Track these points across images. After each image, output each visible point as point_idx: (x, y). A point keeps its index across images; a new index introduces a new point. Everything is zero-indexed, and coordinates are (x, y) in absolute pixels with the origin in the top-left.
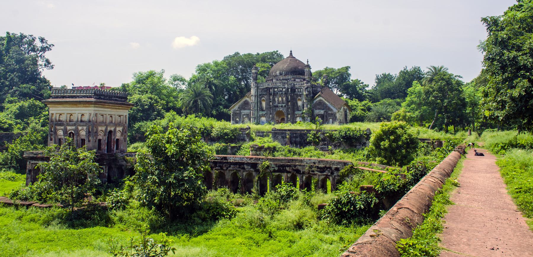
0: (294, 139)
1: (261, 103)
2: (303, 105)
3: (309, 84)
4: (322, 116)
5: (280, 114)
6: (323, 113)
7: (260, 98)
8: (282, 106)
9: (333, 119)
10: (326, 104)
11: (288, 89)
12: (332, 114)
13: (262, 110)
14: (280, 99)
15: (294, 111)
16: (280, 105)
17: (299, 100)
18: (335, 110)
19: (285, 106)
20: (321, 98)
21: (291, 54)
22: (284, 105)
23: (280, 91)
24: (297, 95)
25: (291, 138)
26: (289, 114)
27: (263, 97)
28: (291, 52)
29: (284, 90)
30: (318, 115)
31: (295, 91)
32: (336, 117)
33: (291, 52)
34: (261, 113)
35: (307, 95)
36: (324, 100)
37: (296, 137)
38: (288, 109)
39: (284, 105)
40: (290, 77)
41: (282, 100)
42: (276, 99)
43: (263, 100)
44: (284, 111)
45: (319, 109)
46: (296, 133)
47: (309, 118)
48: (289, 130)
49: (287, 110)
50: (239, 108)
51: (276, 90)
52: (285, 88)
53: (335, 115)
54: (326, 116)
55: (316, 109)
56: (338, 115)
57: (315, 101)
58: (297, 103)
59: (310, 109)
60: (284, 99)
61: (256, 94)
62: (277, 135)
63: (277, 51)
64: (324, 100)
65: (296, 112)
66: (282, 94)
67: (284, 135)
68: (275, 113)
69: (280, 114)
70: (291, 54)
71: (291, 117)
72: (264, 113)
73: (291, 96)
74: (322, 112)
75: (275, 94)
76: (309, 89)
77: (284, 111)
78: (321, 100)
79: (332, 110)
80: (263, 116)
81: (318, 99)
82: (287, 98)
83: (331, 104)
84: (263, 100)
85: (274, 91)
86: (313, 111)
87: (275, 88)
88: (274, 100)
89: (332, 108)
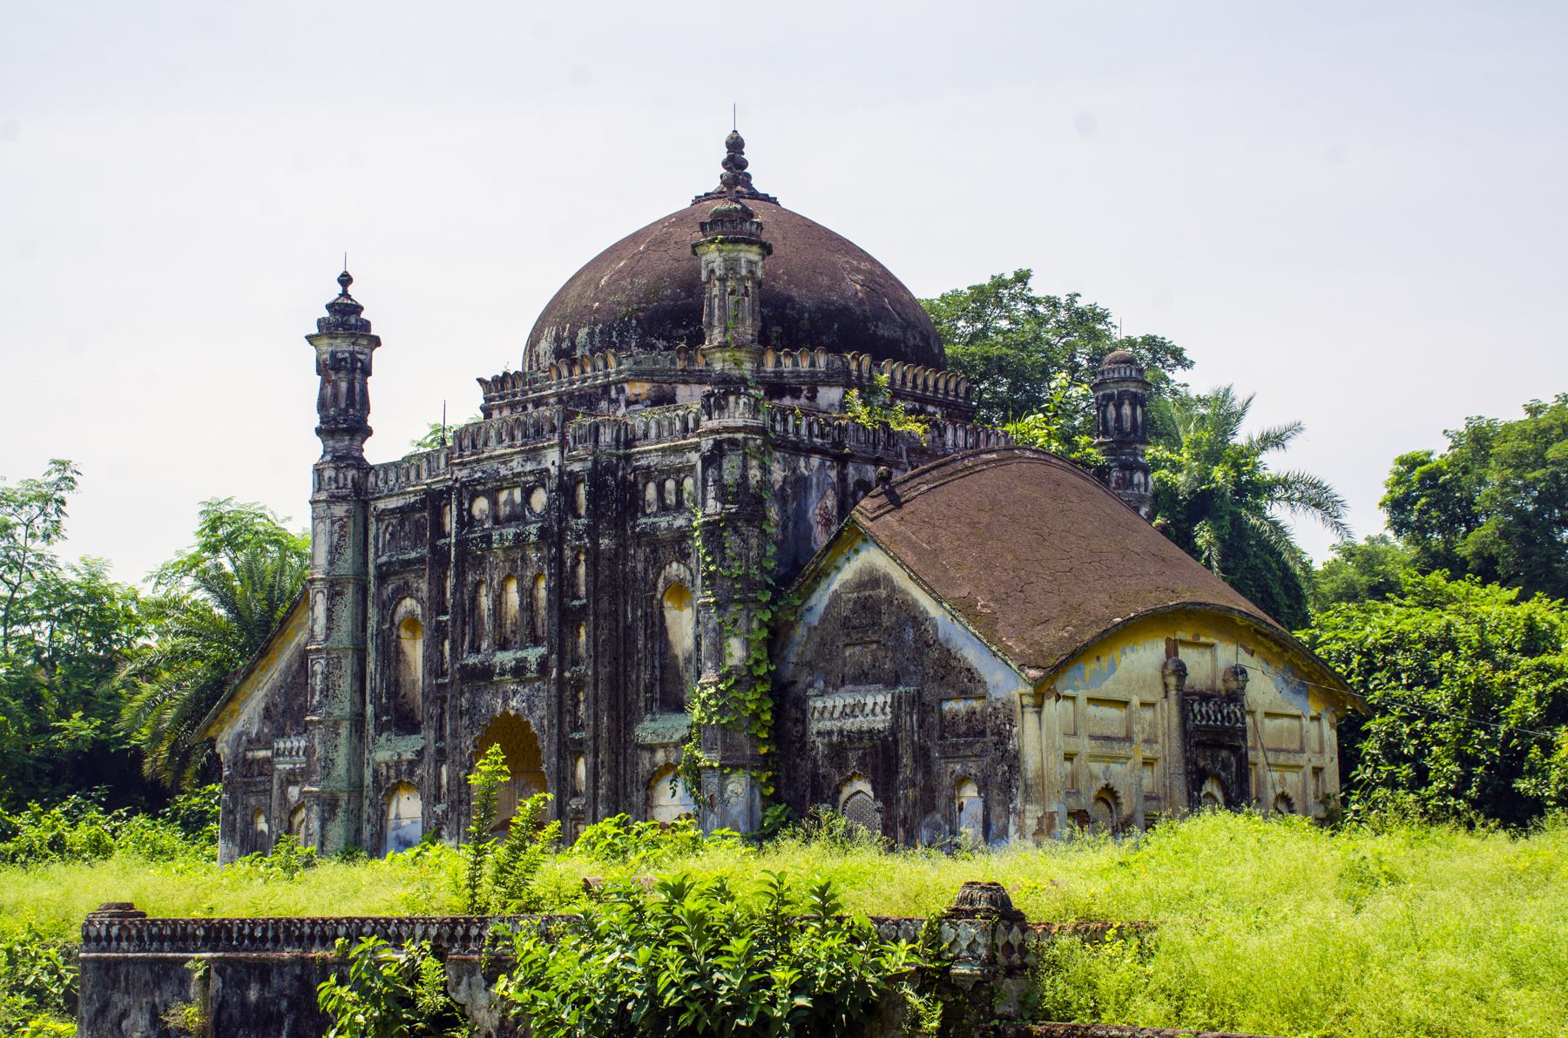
1: (392, 656)
3: (737, 415)
4: (879, 757)
6: (881, 722)
7: (388, 607)
8: (519, 670)
9: (983, 788)
10: (917, 619)
11: (566, 486)
12: (975, 728)
13: (405, 723)
14: (513, 597)
15: (624, 718)
16: (506, 658)
17: (679, 590)
18: (1004, 683)
19: (543, 665)
20: (871, 558)
22: (533, 655)
23: (516, 517)
24: (650, 538)
26: (577, 750)
27: (404, 591)
28: (735, 144)
29: (539, 499)
31: (631, 503)
32: (1014, 761)
33: (735, 144)
34: (388, 750)
35: (713, 531)
38: (566, 693)
39: (533, 655)
40: (615, 366)
41: (528, 606)
42: (485, 602)
44: (539, 717)
45: (862, 678)
46: (263, 971)
47: (737, 785)
48: (216, 933)
49: (563, 709)
50: (267, 714)
51: (481, 505)
53: (1002, 737)
55: (836, 683)
57: (821, 600)
58: (658, 630)
59: (744, 679)
60: (542, 593)
61: (346, 566)
62: (120, 1000)
63: (1022, 277)
64: (900, 577)
65: (648, 729)
66: (520, 540)
71: (594, 774)
72: (407, 747)
73: (594, 557)
74: (872, 709)
75: (471, 557)
76: (730, 468)
78: (872, 580)
79: (970, 684)
81: (847, 572)
82: (563, 587)
83: (964, 608)
84: (412, 623)
85: (467, 521)
86: (786, 703)
87: (470, 490)
88: (468, 612)
89: (972, 654)
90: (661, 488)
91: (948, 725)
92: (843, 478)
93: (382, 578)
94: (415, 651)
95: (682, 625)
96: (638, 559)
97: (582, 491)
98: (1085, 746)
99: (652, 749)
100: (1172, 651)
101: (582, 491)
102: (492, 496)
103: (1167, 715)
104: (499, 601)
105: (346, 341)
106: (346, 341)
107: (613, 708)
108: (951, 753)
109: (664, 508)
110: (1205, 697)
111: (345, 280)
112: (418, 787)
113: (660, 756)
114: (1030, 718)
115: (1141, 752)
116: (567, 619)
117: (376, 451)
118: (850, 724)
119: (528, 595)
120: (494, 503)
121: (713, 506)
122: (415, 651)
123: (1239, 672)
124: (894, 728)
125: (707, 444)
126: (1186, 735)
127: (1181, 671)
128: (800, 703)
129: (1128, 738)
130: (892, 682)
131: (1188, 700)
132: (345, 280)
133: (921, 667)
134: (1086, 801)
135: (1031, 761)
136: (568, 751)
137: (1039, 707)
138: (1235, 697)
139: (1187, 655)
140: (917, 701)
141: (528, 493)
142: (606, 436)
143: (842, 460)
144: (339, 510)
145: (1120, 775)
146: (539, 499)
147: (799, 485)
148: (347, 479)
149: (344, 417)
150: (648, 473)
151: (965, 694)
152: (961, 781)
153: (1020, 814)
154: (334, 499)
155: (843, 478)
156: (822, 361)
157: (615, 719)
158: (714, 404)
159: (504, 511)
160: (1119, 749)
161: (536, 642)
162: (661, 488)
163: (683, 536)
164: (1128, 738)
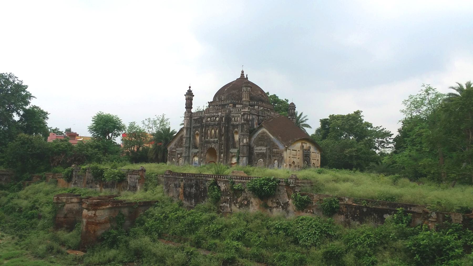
0: (188, 190)
1: (194, 138)
2: (239, 139)
3: (247, 110)
5: (212, 152)
6: (264, 151)
9: (278, 161)
10: (270, 138)
11: (221, 118)
13: (196, 148)
14: (213, 131)
17: (237, 132)
20: (264, 130)
21: (242, 75)
22: (216, 139)
25: (185, 187)
28: (243, 72)
29: (217, 119)
30: (258, 154)
33: (243, 72)
36: (268, 132)
37: (191, 187)
38: (220, 145)
42: (209, 132)
43: (197, 134)
45: (261, 145)
46: (191, 180)
49: (220, 148)
51: (209, 119)
52: (218, 116)
53: (281, 154)
54: (270, 156)
55: (257, 146)
56: (286, 155)
60: (217, 131)
61: (189, 126)
67: (177, 182)
68: (206, 151)
69: (212, 152)
70: (242, 75)
71: (224, 156)
72: (196, 151)
74: (263, 149)
76: (245, 116)
77: (216, 148)
78: (264, 133)
79: (277, 147)
80: (195, 155)
81: (260, 131)
84: (197, 134)
88: (206, 133)
89: (277, 143)
90: (235, 119)
91: (273, 152)
92: (258, 118)
93: (193, 128)
94: (198, 138)
95: (237, 137)
96: (231, 128)
97: (224, 118)
98: (291, 156)
99: (232, 153)
100: (302, 143)
101: (224, 118)
102: (211, 118)
103: (301, 152)
104: (211, 132)
105: (190, 95)
106: (190, 95)
107: (227, 147)
108: (274, 156)
109: (235, 121)
110: (306, 150)
111: (190, 87)
112: (198, 156)
113: (233, 154)
114: (285, 152)
115: (298, 157)
116: (221, 135)
117: (193, 110)
118: (260, 151)
119: (215, 132)
120: (211, 119)
121: (243, 121)
122: (198, 138)
123: (310, 147)
124: (266, 153)
125: (242, 113)
126: (303, 155)
127: (303, 146)
128: (253, 148)
129: (296, 155)
130: (266, 146)
131: (304, 151)
132: (190, 87)
133: (271, 145)
134: (291, 163)
135: (285, 157)
136: (221, 153)
137: (286, 151)
138: (309, 150)
139: (304, 144)
140: (269, 149)
141: (216, 118)
142: (227, 111)
143: (258, 116)
144: (188, 118)
145: (295, 160)
146: (217, 119)
147: (253, 119)
148: (189, 114)
149: (189, 105)
150: (233, 116)
151: (276, 149)
152: (275, 160)
153: (283, 164)
154: (187, 117)
155: (258, 118)
156: (255, 103)
157: (227, 149)
158: (244, 108)
159: (212, 120)
160: (295, 157)
161: (216, 138)
162: (235, 119)
163: (238, 125)
164: (296, 155)
